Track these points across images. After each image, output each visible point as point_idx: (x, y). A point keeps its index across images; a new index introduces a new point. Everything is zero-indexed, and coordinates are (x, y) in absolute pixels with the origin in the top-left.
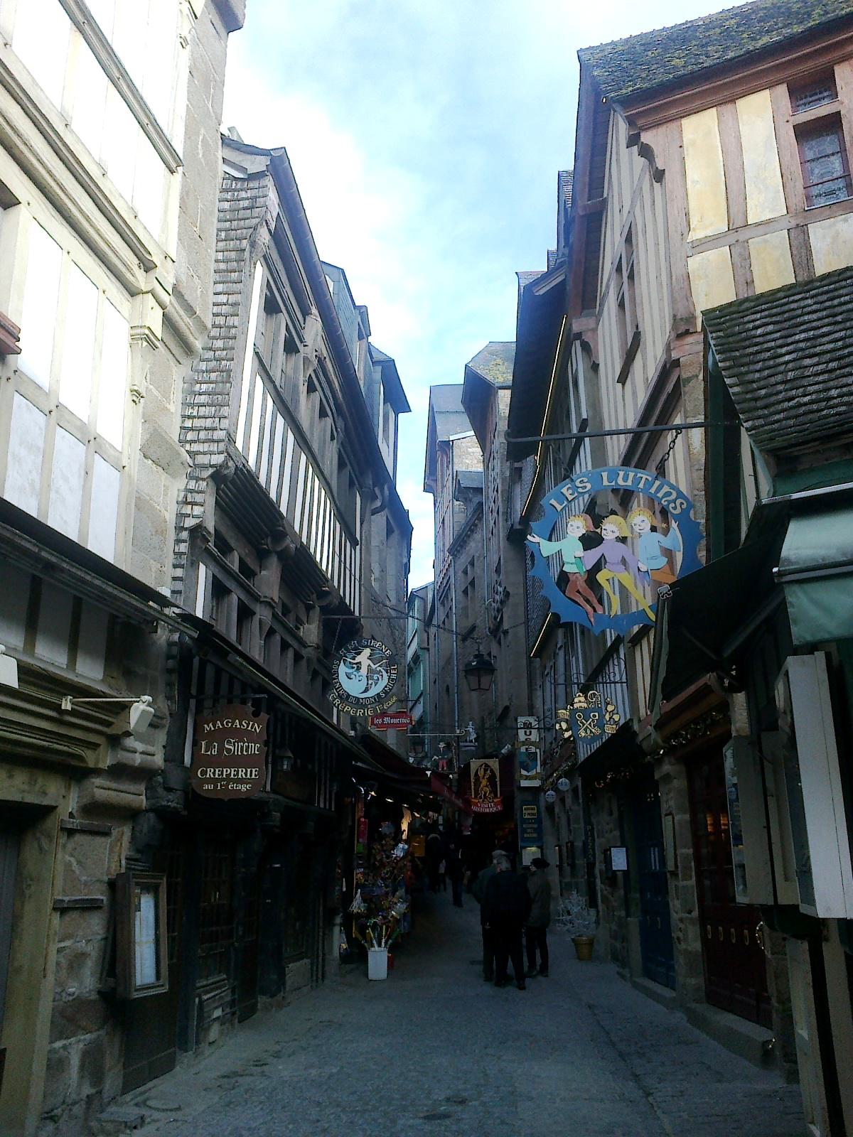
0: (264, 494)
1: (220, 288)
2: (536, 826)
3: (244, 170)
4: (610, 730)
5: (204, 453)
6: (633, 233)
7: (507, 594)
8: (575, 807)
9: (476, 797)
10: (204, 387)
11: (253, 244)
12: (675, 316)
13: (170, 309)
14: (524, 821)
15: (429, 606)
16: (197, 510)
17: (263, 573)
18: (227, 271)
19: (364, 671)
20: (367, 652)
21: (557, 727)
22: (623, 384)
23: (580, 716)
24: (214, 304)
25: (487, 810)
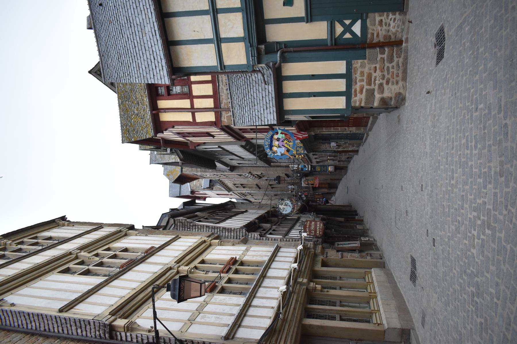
1: (202, 230)
2: (322, 167)
3: (173, 224)
4: (301, 145)
5: (242, 234)
7: (250, 172)
10: (227, 234)
11: (191, 223)
13: (212, 238)
15: (244, 201)
16: (256, 235)
17: (264, 227)
18: (198, 228)
19: (285, 207)
20: (280, 206)
22: (215, 137)
24: (206, 231)
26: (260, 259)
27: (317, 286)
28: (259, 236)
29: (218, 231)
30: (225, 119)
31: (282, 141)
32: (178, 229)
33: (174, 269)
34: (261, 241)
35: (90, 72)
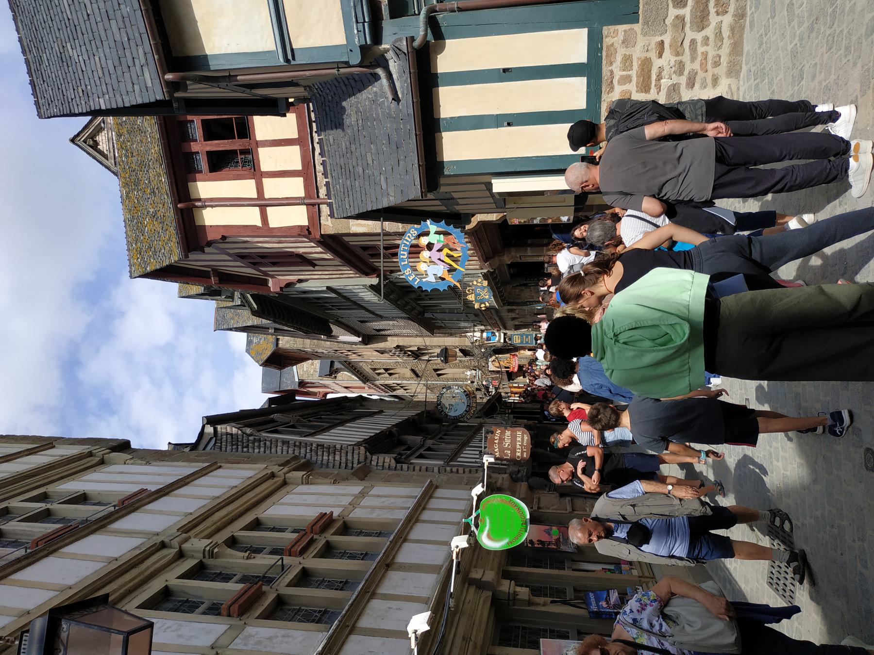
0: (371, 437)
1: (273, 450)
2: (524, 337)
3: (211, 438)
4: (485, 283)
5: (359, 457)
6: (240, 254)
8: (517, 312)
10: (325, 458)
11: (251, 435)
16: (387, 460)
18: (265, 447)
26: (386, 516)
27: (518, 589)
28: (393, 461)
29: (308, 451)
30: (328, 221)
31: (440, 250)
32: (223, 449)
33: (171, 548)
35: (73, 140)
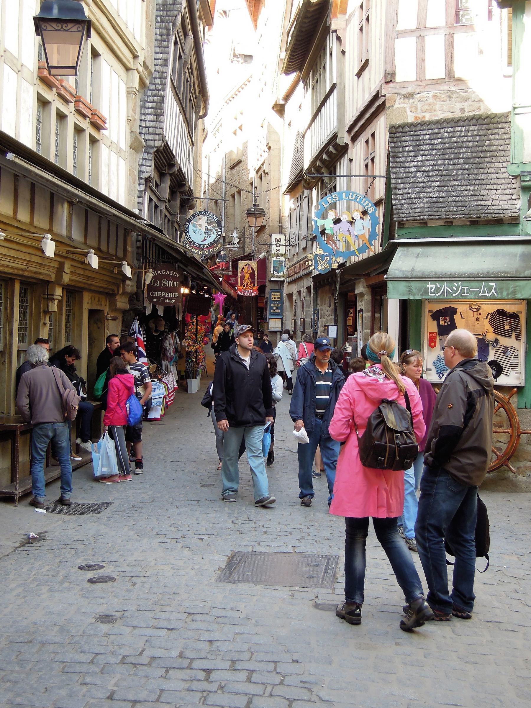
1: (158, 49)
5: (152, 140)
8: (307, 298)
9: (241, 286)
10: (151, 105)
11: (174, 25)
12: (386, 71)
13: (142, 73)
14: (272, 302)
16: (149, 169)
17: (162, 185)
19: (203, 230)
21: (307, 263)
22: (358, 78)
23: (319, 258)
24: (155, 59)
25: (248, 295)
26: (103, 180)
27: (56, 302)
30: (399, 104)
34: (137, 182)
